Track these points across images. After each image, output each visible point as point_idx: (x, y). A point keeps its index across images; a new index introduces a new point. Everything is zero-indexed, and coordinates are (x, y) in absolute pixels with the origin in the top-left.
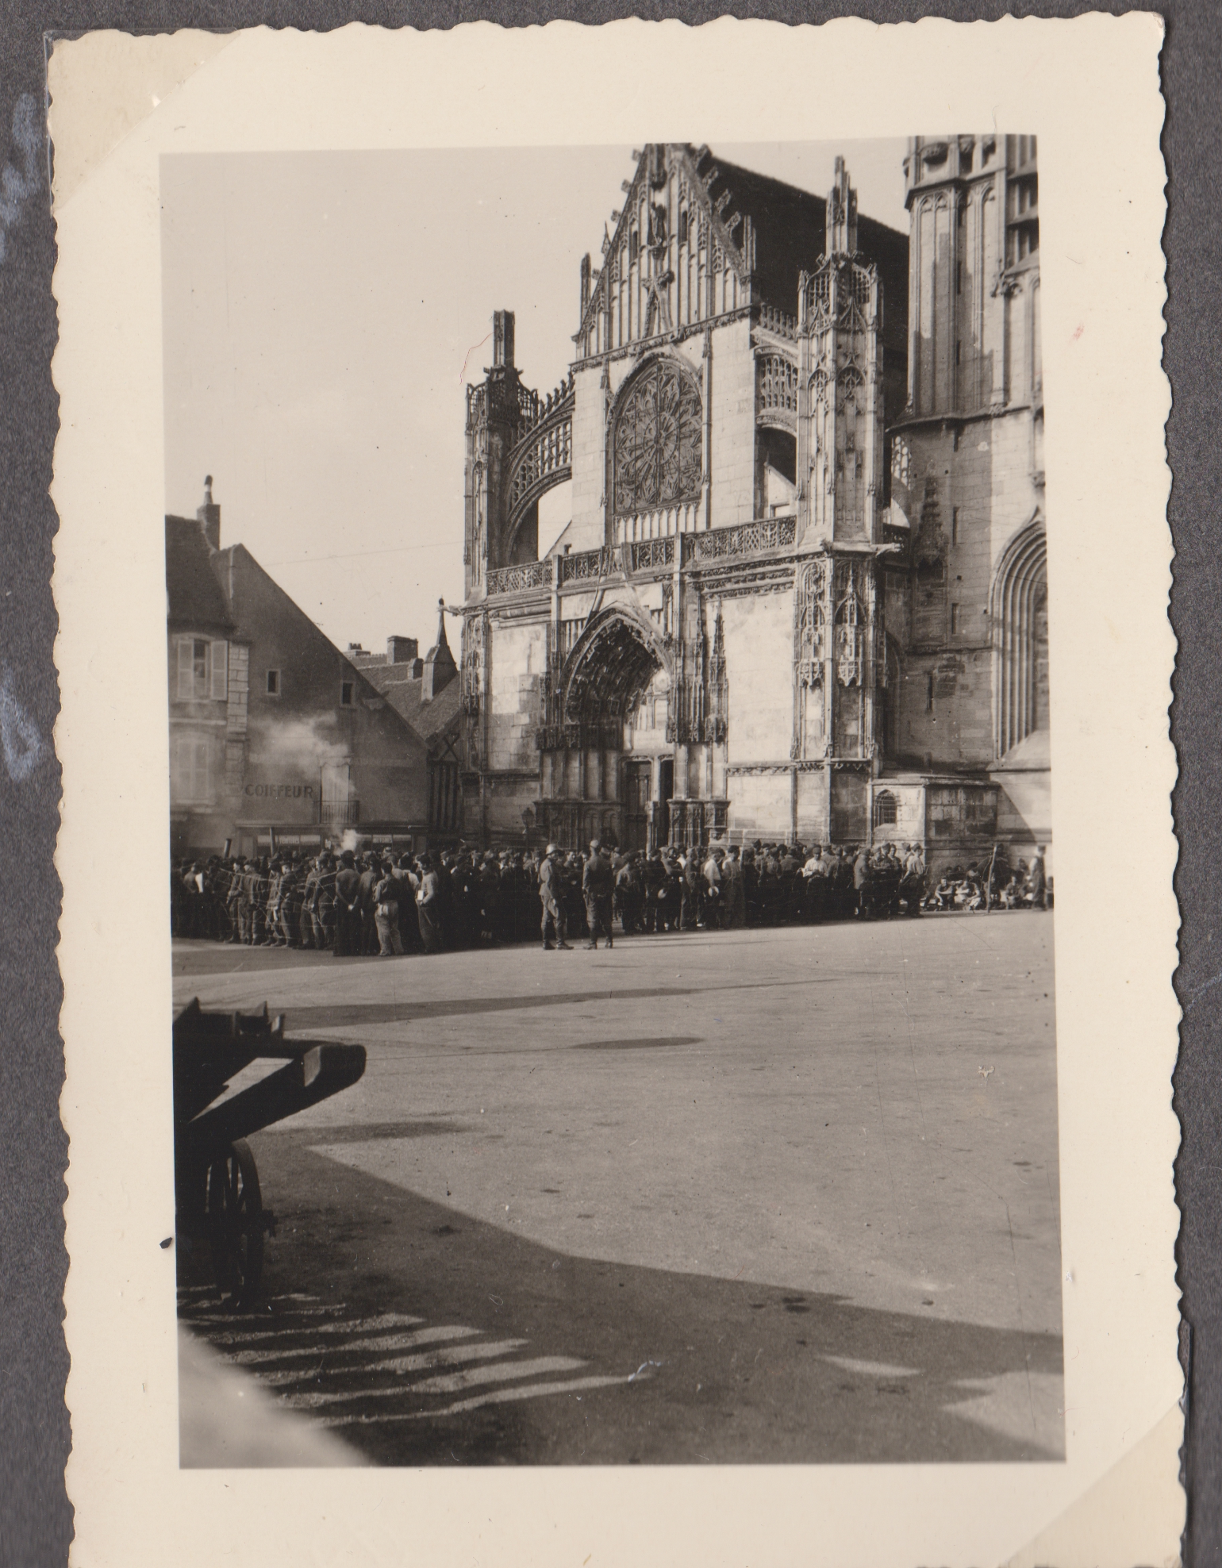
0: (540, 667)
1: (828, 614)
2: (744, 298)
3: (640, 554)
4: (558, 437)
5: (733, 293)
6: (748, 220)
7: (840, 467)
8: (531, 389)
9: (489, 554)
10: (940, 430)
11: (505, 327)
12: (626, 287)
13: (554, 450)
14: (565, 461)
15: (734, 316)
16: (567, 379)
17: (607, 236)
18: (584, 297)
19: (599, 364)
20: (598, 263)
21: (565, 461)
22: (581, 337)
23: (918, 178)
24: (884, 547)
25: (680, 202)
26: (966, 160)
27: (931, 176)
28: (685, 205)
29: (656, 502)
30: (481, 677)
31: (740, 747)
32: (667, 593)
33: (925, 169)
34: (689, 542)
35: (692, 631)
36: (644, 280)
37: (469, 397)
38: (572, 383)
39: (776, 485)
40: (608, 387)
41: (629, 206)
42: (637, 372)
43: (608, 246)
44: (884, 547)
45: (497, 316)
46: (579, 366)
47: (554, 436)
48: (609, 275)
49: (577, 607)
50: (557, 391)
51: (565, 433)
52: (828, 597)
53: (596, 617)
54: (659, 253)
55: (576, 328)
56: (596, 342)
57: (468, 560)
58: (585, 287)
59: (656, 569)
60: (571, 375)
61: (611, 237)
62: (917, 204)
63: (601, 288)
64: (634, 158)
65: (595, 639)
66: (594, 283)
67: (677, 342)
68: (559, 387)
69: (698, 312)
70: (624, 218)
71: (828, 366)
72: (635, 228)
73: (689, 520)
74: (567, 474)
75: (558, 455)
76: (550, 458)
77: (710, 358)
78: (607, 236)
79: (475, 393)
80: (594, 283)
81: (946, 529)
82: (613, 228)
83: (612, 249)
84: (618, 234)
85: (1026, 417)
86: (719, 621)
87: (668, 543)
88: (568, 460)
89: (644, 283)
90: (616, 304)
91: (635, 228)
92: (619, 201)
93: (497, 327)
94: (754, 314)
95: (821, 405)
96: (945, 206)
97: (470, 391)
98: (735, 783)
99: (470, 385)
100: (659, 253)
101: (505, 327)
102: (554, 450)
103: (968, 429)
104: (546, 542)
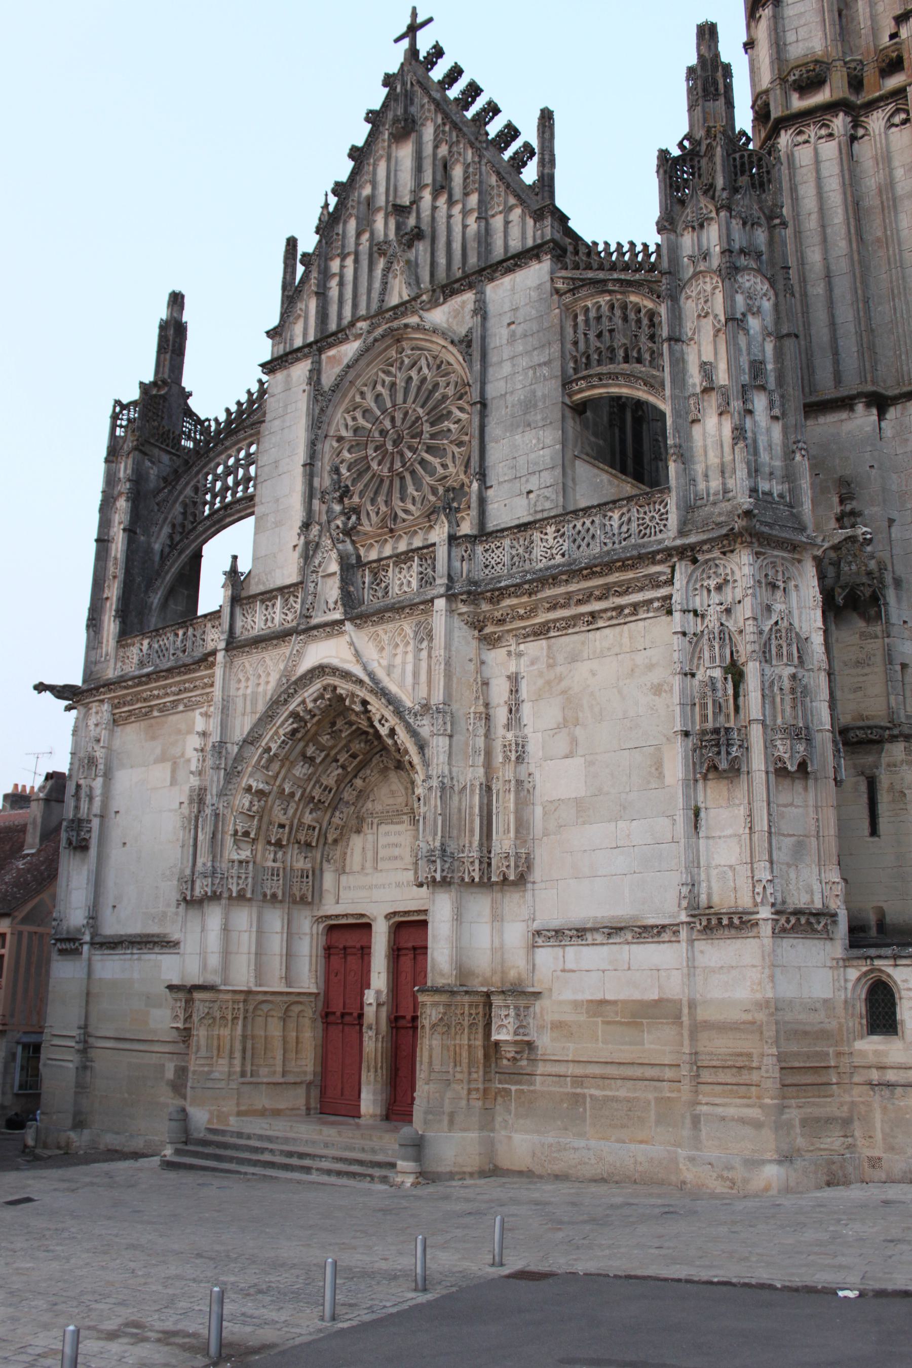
4: (238, 460)
8: (203, 418)
9: (123, 614)
10: (851, 408)
12: (349, 261)
17: (326, 205)
18: (287, 285)
25: (436, 147)
28: (443, 150)
30: (98, 791)
33: (795, 96)
36: (378, 244)
37: (115, 417)
40: (319, 379)
43: (326, 218)
50: (239, 404)
51: (248, 455)
57: (94, 623)
61: (331, 209)
65: (286, 720)
66: (300, 269)
72: (367, 191)
76: (226, 488)
77: (484, 318)
78: (326, 205)
82: (333, 201)
88: (251, 490)
90: (334, 283)
97: (118, 409)
99: (118, 402)
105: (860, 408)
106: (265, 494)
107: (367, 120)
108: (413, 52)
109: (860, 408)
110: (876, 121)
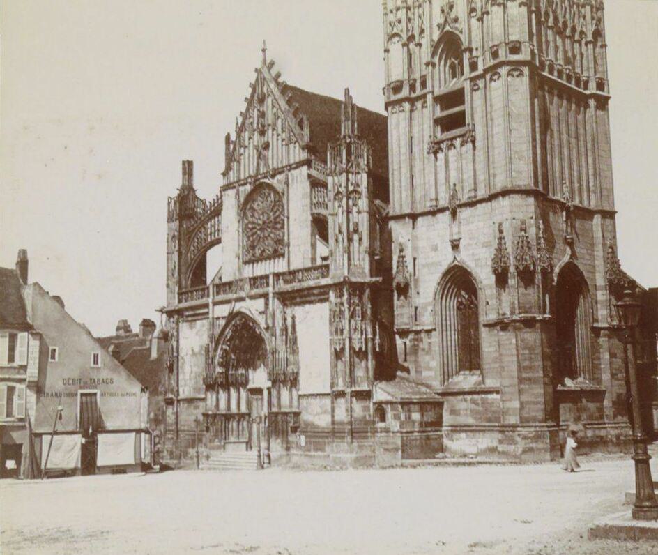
0: (205, 340)
1: (347, 315)
2: (304, 155)
3: (254, 281)
5: (298, 154)
6: (305, 118)
7: (350, 240)
8: (202, 199)
11: (188, 168)
13: (213, 229)
14: (218, 235)
15: (299, 165)
16: (219, 194)
17: (237, 124)
19: (234, 187)
20: (233, 137)
21: (218, 235)
22: (225, 174)
23: (389, 98)
24: (374, 279)
26: (413, 88)
27: (394, 97)
29: (262, 258)
31: (305, 386)
32: (267, 304)
34: (277, 275)
35: (279, 323)
37: (169, 203)
38: (221, 196)
39: (322, 250)
41: (248, 110)
42: (253, 191)
43: (238, 130)
44: (374, 279)
45: (184, 163)
46: (225, 188)
47: (213, 221)
48: (239, 143)
49: (223, 311)
50: (214, 200)
52: (346, 305)
53: (232, 316)
54: (262, 133)
55: (223, 169)
56: (232, 176)
58: (227, 148)
59: (260, 291)
60: (221, 192)
61: (239, 125)
62: (390, 109)
63: (234, 148)
64: (250, 86)
66: (232, 146)
67: (273, 177)
68: (215, 198)
69: (281, 162)
70: (245, 116)
71: (342, 190)
73: (280, 266)
74: (218, 241)
75: (215, 231)
76: (211, 233)
79: (173, 201)
80: (232, 146)
81: (410, 268)
82: (240, 120)
83: (241, 130)
84: (243, 124)
85: (448, 213)
86: (293, 318)
87: (267, 277)
89: (256, 148)
91: (251, 120)
92: (243, 107)
93: (184, 169)
94: (308, 163)
95: (340, 209)
96: (403, 110)
98: (304, 402)
99: (169, 197)
100: (262, 133)
101: (188, 168)
102: (213, 229)
103: (420, 219)
104: (210, 275)
105: (407, 218)
106: (225, 238)
107: (250, 86)
108: (264, 60)
109: (407, 218)
110: (419, 104)
